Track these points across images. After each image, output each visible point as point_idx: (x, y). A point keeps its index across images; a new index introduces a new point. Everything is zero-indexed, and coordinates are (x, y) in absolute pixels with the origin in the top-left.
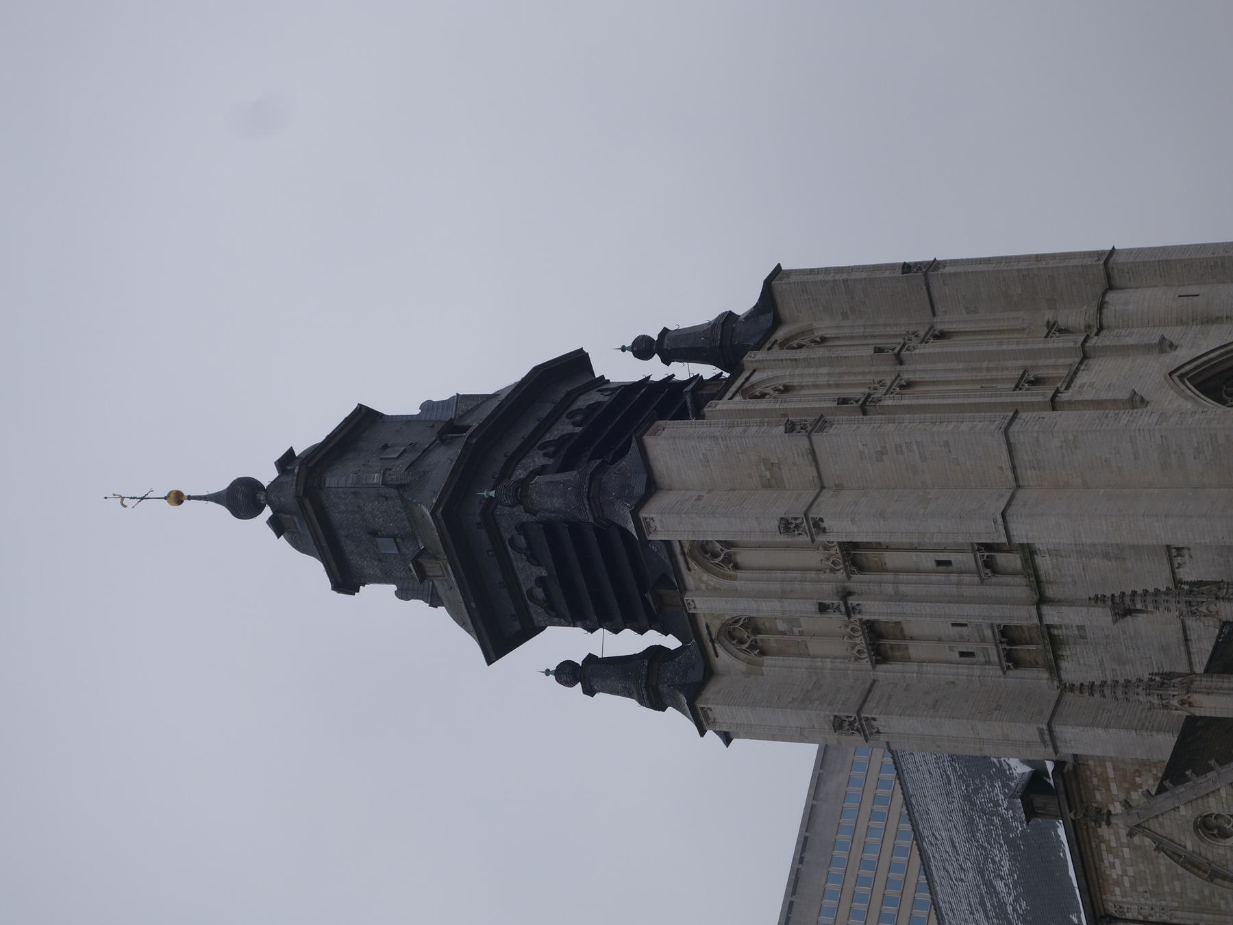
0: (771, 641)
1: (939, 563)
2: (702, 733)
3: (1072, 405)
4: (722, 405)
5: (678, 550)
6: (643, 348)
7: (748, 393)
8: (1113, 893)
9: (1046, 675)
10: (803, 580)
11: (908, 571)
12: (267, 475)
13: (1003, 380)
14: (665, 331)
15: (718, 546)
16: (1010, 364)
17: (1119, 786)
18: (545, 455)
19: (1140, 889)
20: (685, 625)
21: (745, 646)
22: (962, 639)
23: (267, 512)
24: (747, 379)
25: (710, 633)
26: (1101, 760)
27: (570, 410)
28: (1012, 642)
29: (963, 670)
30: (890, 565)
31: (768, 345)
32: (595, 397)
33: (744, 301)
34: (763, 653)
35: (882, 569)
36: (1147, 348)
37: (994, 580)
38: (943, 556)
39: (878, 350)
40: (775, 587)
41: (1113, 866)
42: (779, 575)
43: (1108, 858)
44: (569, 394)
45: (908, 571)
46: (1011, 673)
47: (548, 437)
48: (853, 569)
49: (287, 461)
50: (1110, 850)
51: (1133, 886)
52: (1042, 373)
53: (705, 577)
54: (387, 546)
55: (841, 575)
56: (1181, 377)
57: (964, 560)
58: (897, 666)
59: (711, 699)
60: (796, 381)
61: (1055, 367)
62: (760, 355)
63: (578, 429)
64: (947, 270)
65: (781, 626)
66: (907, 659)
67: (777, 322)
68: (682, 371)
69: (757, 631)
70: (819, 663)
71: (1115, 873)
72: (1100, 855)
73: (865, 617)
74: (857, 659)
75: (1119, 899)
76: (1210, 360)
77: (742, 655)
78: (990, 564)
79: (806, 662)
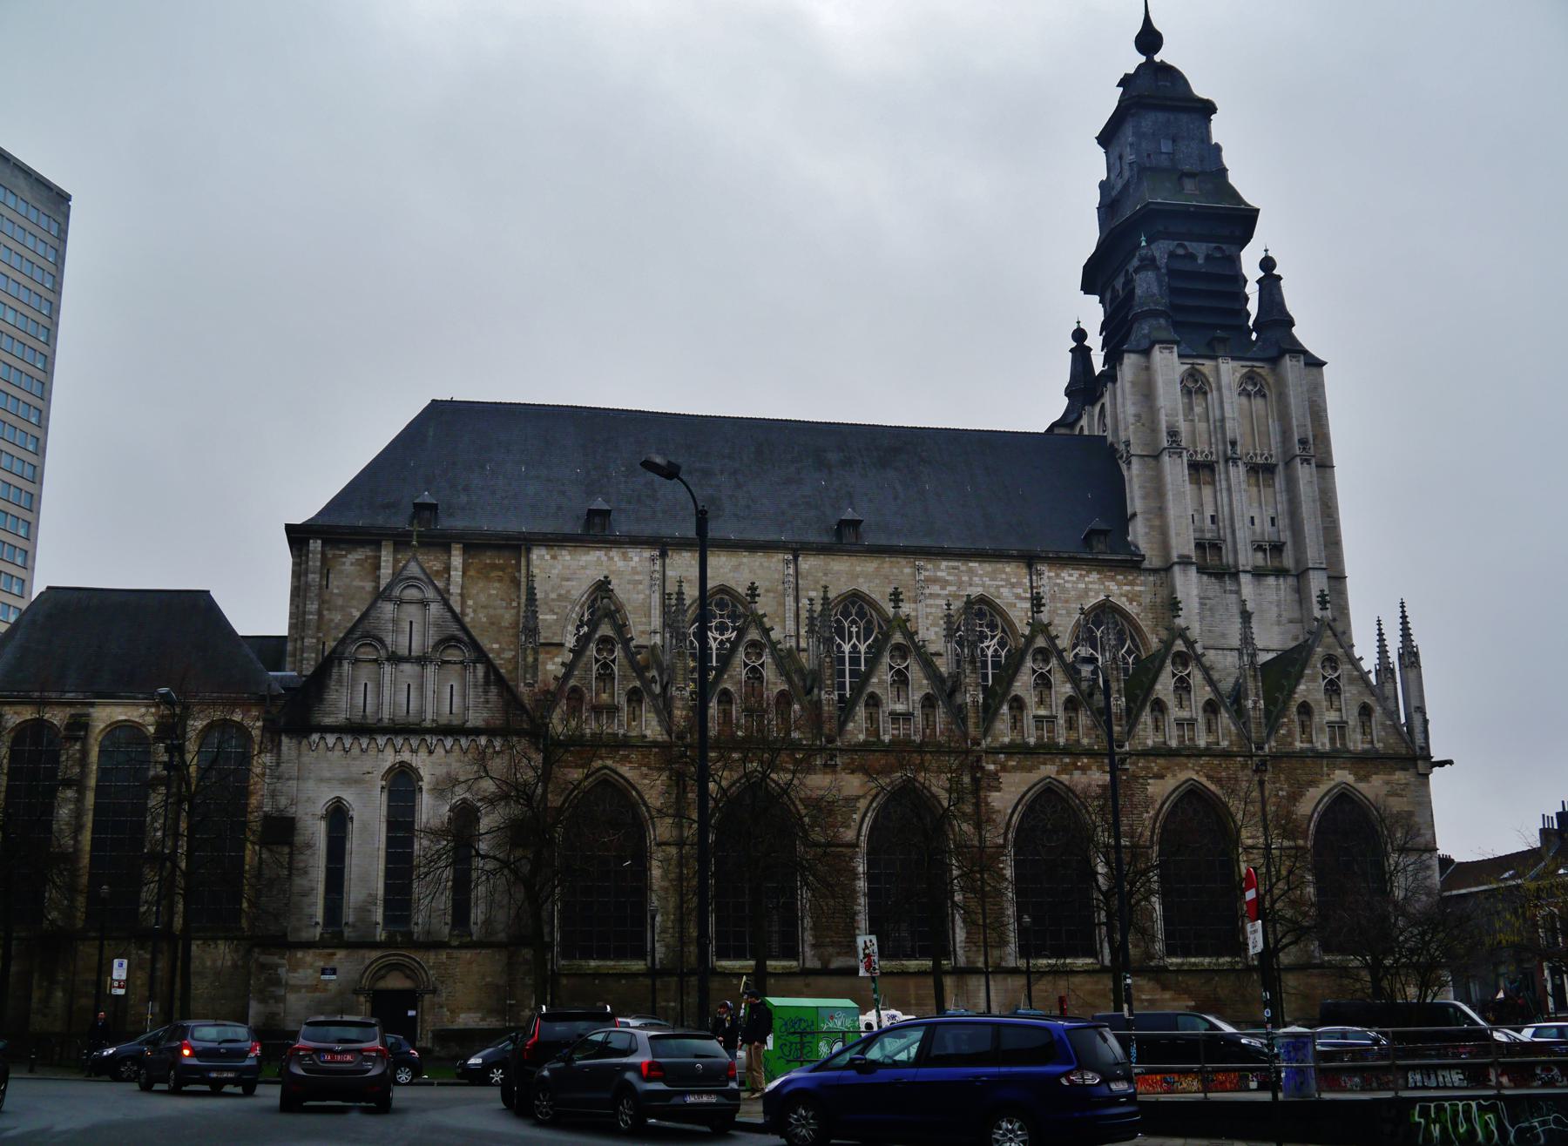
17: (1128, 591)
19: (1056, 589)
41: (1071, 575)
43: (1076, 574)
51: (1059, 585)
71: (1064, 574)
75: (1046, 574)
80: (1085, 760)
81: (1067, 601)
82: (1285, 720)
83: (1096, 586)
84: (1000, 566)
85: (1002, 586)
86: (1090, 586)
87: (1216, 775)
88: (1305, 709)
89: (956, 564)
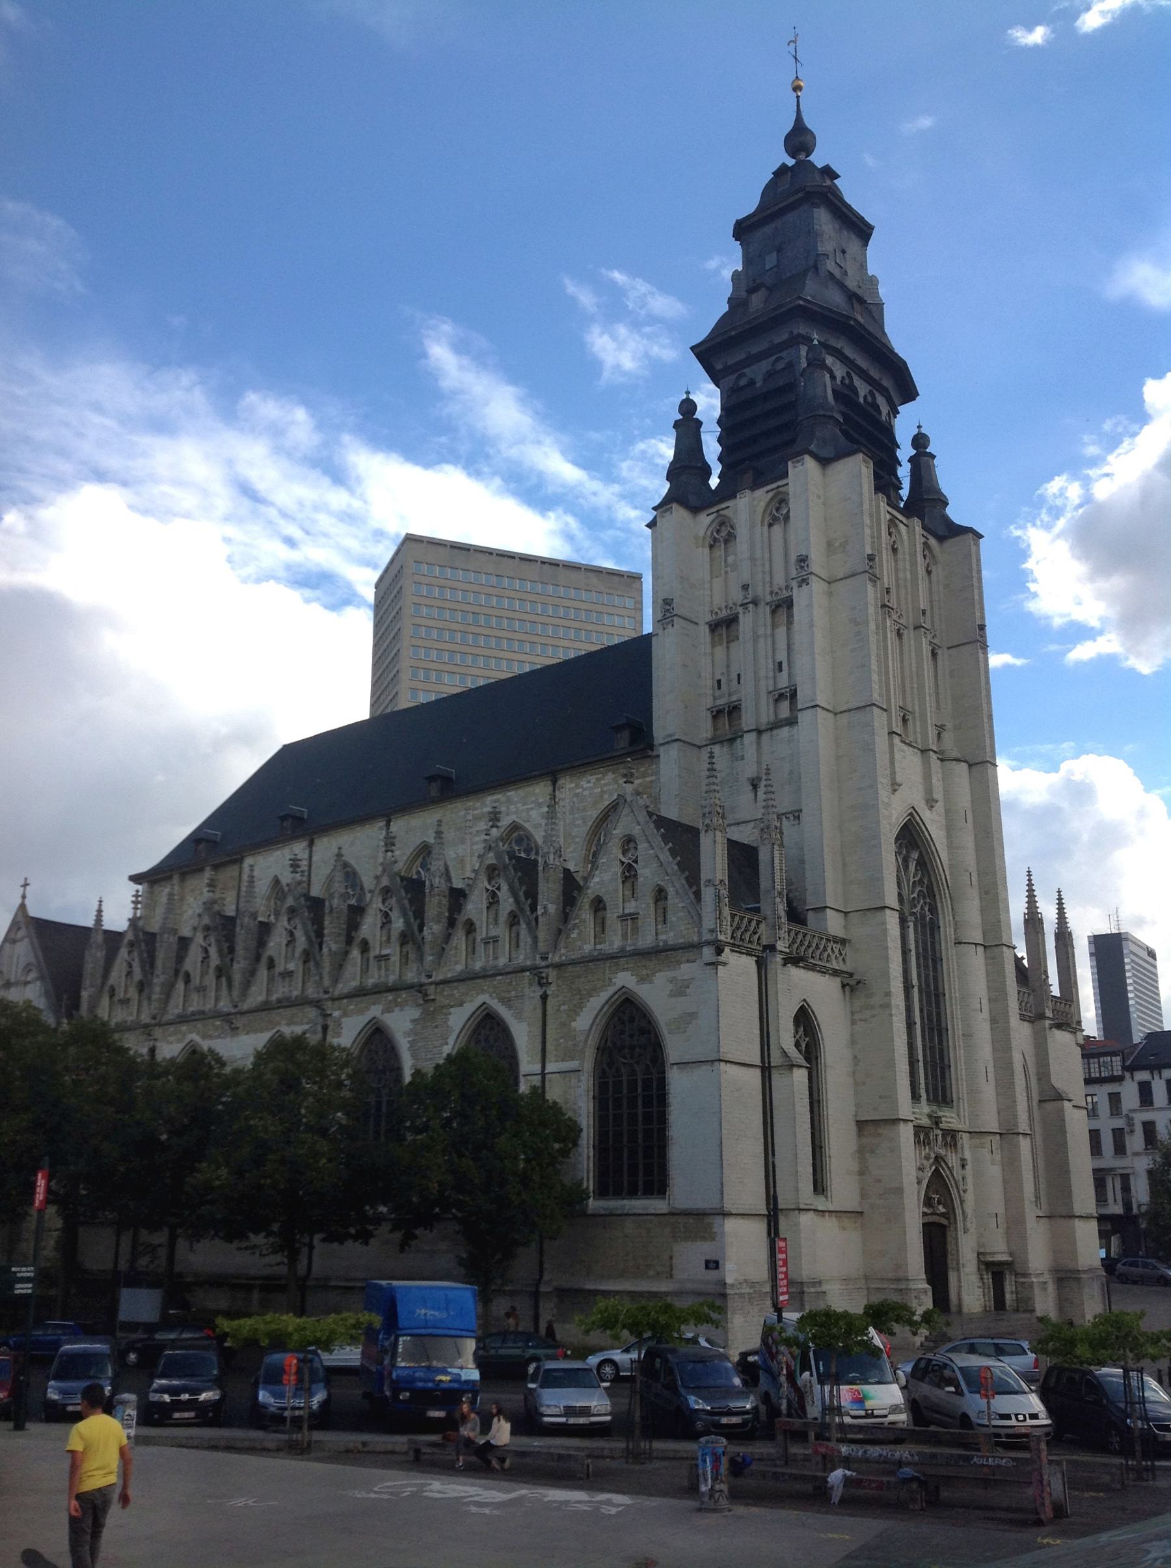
0: (720, 551)
1: (780, 664)
2: (655, 509)
3: (891, 745)
4: (883, 506)
5: (781, 483)
6: (920, 441)
7: (892, 522)
8: (571, 782)
9: (709, 735)
10: (763, 572)
11: (774, 643)
12: (818, 159)
13: (904, 698)
14: (933, 457)
15: (784, 512)
16: (916, 702)
17: (640, 785)
18: (843, 377)
19: (575, 799)
20: (728, 490)
21: (715, 534)
22: (729, 681)
23: (791, 162)
24: (901, 522)
25: (722, 509)
26: (657, 773)
27: (875, 392)
28: (730, 713)
29: (709, 683)
30: (777, 631)
31: (925, 534)
32: (885, 409)
33: (956, 513)
34: (711, 547)
35: (774, 626)
36: (929, 790)
37: (771, 700)
38: (785, 666)
39: (924, 612)
40: (758, 554)
41: (589, 782)
42: (767, 556)
43: (593, 779)
44: (886, 390)
45: (774, 643)
46: (709, 713)
47: (855, 378)
48: (774, 607)
49: (829, 173)
50: (598, 780)
51: (577, 795)
52: (910, 723)
53: (763, 504)
54: (771, 260)
55: (768, 598)
56: (911, 814)
57: (783, 681)
58: (708, 639)
59: (679, 513)
60: (900, 556)
61: (915, 733)
62: (918, 529)
63: (861, 400)
64: (981, 656)
65: (731, 559)
66: (713, 645)
67: (941, 539)
68: (904, 472)
69: (726, 542)
70: (707, 586)
72: (595, 774)
73: (741, 616)
74: (712, 612)
75: (568, 786)
76: (923, 833)
77: (709, 533)
78: (781, 697)
79: (707, 577)
80: (404, 996)
81: (584, 810)
82: (577, 921)
83: (611, 787)
84: (530, 789)
85: (532, 809)
86: (606, 789)
87: (507, 995)
88: (599, 905)
89: (495, 797)
